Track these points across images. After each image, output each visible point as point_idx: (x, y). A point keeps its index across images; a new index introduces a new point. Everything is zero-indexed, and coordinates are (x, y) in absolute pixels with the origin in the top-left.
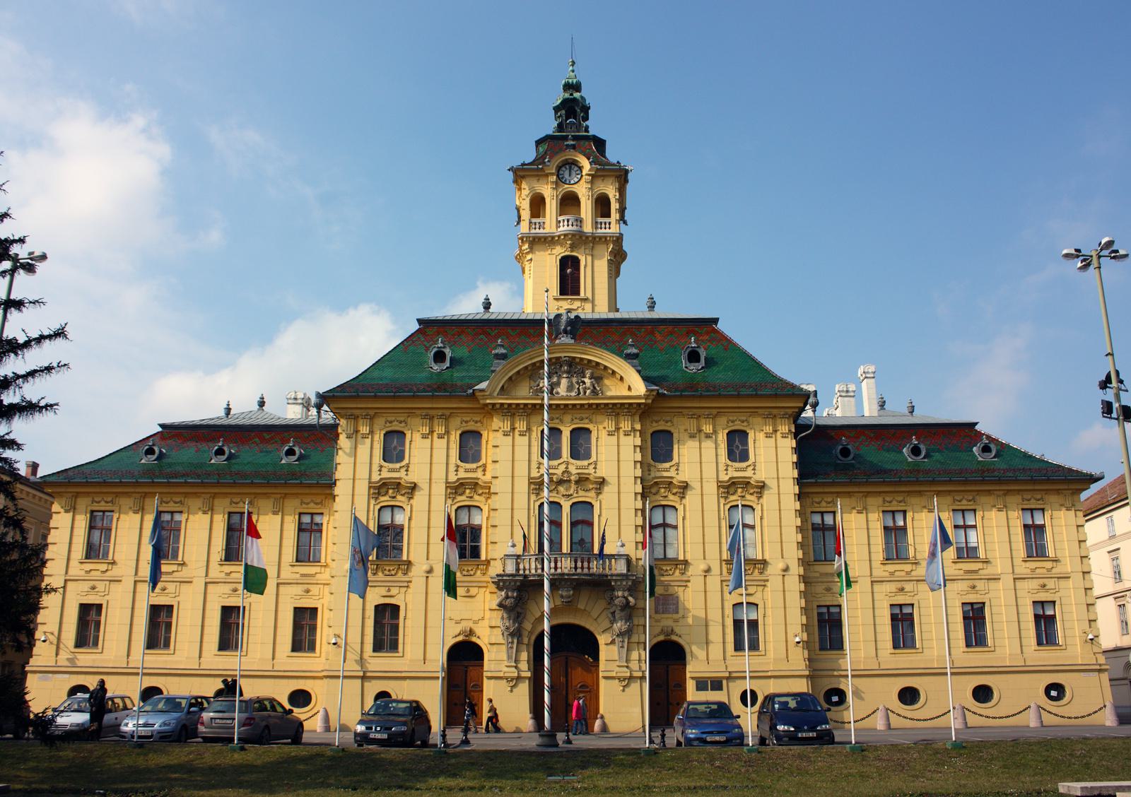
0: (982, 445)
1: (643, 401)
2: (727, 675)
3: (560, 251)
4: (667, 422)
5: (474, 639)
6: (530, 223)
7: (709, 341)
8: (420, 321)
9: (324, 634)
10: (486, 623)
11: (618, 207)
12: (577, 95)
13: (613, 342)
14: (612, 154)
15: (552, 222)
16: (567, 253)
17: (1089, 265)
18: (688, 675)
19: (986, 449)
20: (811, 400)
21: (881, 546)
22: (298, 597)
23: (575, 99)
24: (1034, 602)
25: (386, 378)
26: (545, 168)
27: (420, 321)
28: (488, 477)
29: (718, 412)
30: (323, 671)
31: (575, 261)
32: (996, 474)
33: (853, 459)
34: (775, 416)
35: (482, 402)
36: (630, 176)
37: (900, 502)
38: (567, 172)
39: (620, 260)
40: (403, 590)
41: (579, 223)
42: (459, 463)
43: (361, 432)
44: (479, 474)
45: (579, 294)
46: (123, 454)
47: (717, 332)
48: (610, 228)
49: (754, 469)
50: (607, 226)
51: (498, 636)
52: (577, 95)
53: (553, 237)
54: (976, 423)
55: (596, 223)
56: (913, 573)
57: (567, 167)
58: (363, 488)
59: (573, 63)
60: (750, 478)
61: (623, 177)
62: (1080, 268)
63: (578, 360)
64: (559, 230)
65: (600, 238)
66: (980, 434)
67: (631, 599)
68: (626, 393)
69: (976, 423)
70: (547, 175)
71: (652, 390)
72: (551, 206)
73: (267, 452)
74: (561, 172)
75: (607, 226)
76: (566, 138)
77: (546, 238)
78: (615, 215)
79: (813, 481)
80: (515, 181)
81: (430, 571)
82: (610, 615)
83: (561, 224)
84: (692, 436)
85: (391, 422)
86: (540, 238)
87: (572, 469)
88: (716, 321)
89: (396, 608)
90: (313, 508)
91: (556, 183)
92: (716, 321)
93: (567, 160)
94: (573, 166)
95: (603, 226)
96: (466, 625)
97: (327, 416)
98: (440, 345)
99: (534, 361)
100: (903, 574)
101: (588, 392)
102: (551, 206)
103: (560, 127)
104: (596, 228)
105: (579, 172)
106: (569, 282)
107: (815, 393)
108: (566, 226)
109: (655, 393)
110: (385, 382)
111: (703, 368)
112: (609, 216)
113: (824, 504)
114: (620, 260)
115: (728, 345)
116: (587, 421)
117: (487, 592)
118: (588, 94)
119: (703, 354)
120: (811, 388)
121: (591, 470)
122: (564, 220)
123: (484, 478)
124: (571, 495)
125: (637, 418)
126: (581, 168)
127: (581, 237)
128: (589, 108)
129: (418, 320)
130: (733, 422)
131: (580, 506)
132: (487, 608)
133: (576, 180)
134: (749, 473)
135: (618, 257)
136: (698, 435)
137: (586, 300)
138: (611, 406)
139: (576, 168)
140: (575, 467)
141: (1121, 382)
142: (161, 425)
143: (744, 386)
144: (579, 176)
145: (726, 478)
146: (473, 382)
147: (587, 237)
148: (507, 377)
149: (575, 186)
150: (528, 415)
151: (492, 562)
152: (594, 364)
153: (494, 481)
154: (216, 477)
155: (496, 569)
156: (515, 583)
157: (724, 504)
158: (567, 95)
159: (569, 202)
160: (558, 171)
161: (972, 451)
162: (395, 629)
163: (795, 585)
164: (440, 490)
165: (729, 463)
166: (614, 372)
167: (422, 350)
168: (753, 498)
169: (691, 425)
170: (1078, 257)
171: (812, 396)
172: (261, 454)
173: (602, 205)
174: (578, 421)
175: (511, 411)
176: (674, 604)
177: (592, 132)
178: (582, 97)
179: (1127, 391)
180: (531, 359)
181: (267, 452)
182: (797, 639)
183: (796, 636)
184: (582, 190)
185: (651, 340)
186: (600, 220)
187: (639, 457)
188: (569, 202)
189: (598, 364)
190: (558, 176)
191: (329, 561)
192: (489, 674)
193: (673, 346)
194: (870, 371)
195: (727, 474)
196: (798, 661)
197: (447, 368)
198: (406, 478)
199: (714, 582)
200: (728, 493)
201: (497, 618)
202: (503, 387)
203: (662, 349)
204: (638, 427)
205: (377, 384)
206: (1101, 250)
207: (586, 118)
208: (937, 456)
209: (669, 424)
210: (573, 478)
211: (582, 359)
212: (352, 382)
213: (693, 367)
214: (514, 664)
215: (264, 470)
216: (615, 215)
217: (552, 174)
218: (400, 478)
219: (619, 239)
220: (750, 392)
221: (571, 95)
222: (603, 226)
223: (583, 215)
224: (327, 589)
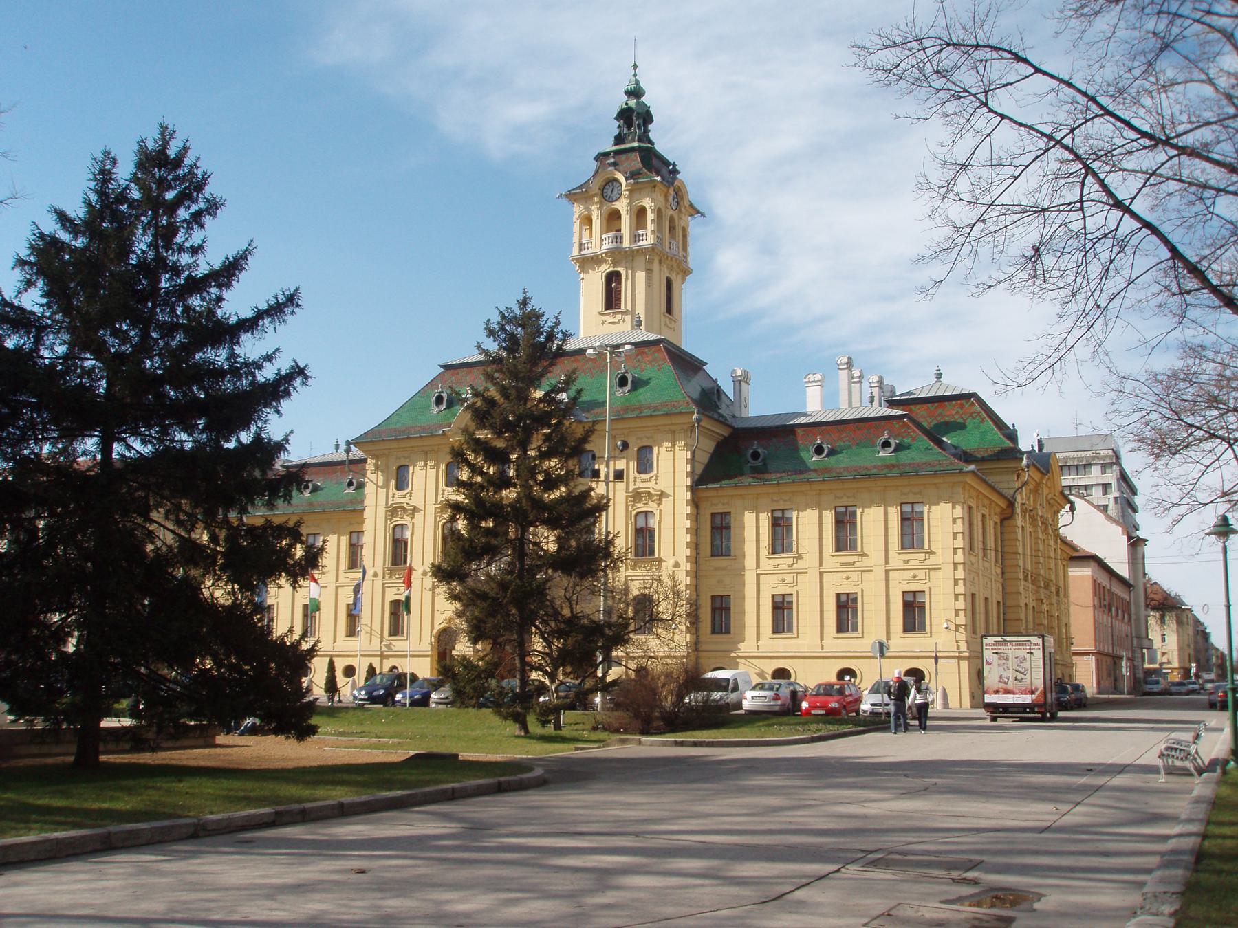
3: (605, 268)
16: (611, 269)
31: (618, 274)
56: (794, 566)
59: (635, 67)
64: (583, 253)
77: (592, 257)
86: (588, 258)
91: (601, 202)
97: (356, 452)
100: (786, 567)
127: (620, 253)
137: (625, 312)
147: (626, 252)
159: (613, 218)
184: (622, 205)
217: (596, 195)
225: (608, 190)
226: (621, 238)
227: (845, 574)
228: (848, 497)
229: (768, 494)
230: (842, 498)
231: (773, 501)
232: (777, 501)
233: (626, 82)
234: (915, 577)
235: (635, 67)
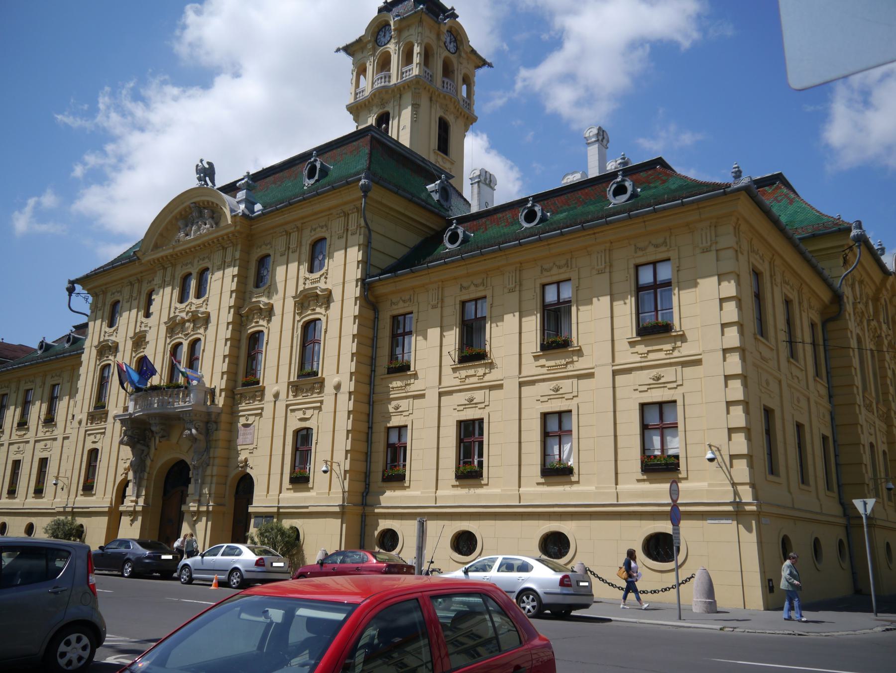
1: (232, 229)
16: (381, 111)
29: (302, 224)
111: (317, 181)
127: (387, 92)
147: (393, 91)
168: (322, 311)
174: (201, 262)
226: (390, 77)
227: (553, 384)
228: (559, 267)
230: (550, 270)
234: (658, 379)
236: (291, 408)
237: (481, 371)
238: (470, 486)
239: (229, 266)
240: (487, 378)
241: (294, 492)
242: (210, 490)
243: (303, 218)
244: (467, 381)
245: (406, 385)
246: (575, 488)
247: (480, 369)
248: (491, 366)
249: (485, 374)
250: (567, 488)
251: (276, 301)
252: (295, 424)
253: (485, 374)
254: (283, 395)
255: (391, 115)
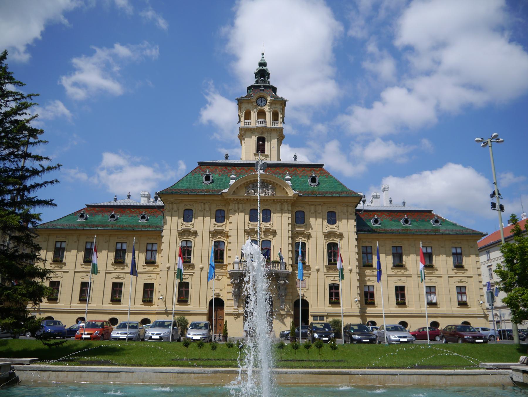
0: (435, 220)
1: (292, 198)
2: (326, 314)
4: (302, 207)
5: (220, 297)
6: (245, 123)
7: (320, 174)
8: (199, 163)
9: (157, 296)
10: (225, 291)
11: (281, 117)
12: (264, 68)
13: (280, 173)
14: (279, 94)
15: (254, 122)
16: (260, 136)
17: (486, 145)
18: (310, 314)
19: (436, 221)
20: (363, 199)
21: (391, 261)
22: (146, 279)
23: (264, 70)
24: (457, 287)
25: (185, 186)
26: (251, 99)
27: (199, 163)
28: (227, 229)
30: (156, 311)
32: (441, 232)
33: (380, 224)
34: (347, 206)
35: (226, 197)
36: (287, 103)
37: (399, 243)
38: (261, 101)
39: (282, 139)
40: (191, 276)
41: (265, 123)
42: (215, 223)
43: (174, 209)
44: (223, 228)
45: (264, 153)
46: (71, 217)
47: (323, 170)
48: (278, 125)
49: (338, 228)
50: (277, 124)
51: (230, 296)
52: (264, 68)
53: (254, 129)
54: (432, 210)
55: (272, 123)
57: (261, 99)
58: (174, 233)
59: (263, 54)
60: (337, 231)
61: (284, 104)
62: (483, 146)
63: (265, 181)
65: (274, 130)
66: (434, 215)
67: (287, 281)
68: (285, 195)
69: (432, 210)
70: (252, 102)
71: (296, 194)
72: (254, 114)
73: (133, 217)
74: (258, 101)
75: (277, 124)
76: (260, 87)
77: (251, 129)
78: (280, 120)
79: (363, 233)
80: (238, 104)
81: (202, 269)
82: (278, 288)
83: (258, 123)
84: (313, 213)
85: (187, 205)
87: (262, 226)
88: (322, 165)
89: (187, 284)
90: (152, 241)
91: (256, 106)
92: (322, 165)
93: (260, 96)
94: (263, 99)
95: (275, 124)
96: (217, 292)
97: (159, 203)
98: (208, 173)
99: (247, 181)
101: (270, 194)
102: (254, 114)
103: (257, 82)
104: (272, 125)
105: (265, 101)
106: (261, 148)
107: (365, 197)
108: (260, 124)
109: (297, 195)
110: (184, 188)
111: (317, 185)
112: (277, 120)
113: (367, 243)
114: (282, 139)
115: (328, 175)
116: (269, 206)
117: (226, 277)
118: (269, 68)
119: (317, 179)
120: (362, 194)
121: (270, 227)
122: (259, 122)
123: (225, 230)
124: (262, 237)
125: (290, 205)
126: (266, 100)
127: (266, 129)
128: (270, 74)
129: (198, 163)
130: (329, 208)
131: (265, 242)
132: (226, 284)
133: (264, 104)
134: (336, 229)
135: (281, 138)
136: (315, 213)
138: (279, 200)
139: (264, 100)
140: (264, 225)
141: (499, 194)
142: (86, 205)
143: (334, 193)
144: (265, 103)
145: (327, 231)
146: (221, 189)
147: (268, 129)
148: (236, 187)
149: (264, 107)
150: (245, 203)
151: (228, 265)
152: (272, 183)
153: (230, 231)
154: (111, 227)
155: (230, 268)
156: (285, 274)
157: (326, 242)
158: (261, 68)
159: (261, 114)
160: (257, 101)
161: (430, 222)
162: (187, 293)
163: (355, 277)
164: (207, 234)
165: (328, 225)
166: (280, 186)
167: (200, 175)
169: (313, 209)
170: (482, 141)
171: (363, 197)
172: (131, 218)
173: (275, 116)
174: (264, 206)
175: (238, 201)
176: (304, 284)
177: (271, 84)
178: (267, 69)
179: (502, 198)
180: (246, 180)
181: (133, 217)
182: (356, 300)
183: (355, 298)
184: (267, 108)
185: (296, 173)
186: (274, 121)
187: (290, 222)
188: (261, 114)
189: (274, 182)
190: (257, 102)
191: (159, 264)
192: (227, 312)
193: (305, 175)
194: (386, 187)
195: (327, 230)
196: (356, 309)
197: (211, 183)
198: (193, 229)
199: (321, 274)
200: (327, 237)
201: (231, 289)
202: (234, 191)
203: (300, 177)
204: (290, 208)
205: (181, 189)
206: (492, 139)
207: (268, 78)
208: (415, 224)
209: (303, 208)
210: (263, 230)
211: (267, 180)
212: (170, 188)
213: (313, 185)
214: (237, 308)
215: (132, 224)
216: (280, 120)
217: (254, 102)
218: (191, 229)
219: (282, 130)
220: (337, 195)
221: (263, 68)
222: (275, 124)
223: (267, 120)
224: (158, 276)
225: (259, 101)
229: (391, 239)
231: (393, 242)
232: (395, 242)
233: (259, 60)
235: (263, 54)
236: (326, 275)
237: (403, 271)
238: (402, 307)
239: (285, 212)
240: (405, 273)
241: (332, 307)
242: (289, 306)
243: (324, 202)
244: (397, 273)
245: (372, 272)
246: (439, 309)
247: (402, 270)
248: (406, 270)
249: (404, 272)
250: (436, 309)
251: (312, 232)
252: (329, 281)
253: (404, 272)
254: (321, 270)
255: (266, 140)
